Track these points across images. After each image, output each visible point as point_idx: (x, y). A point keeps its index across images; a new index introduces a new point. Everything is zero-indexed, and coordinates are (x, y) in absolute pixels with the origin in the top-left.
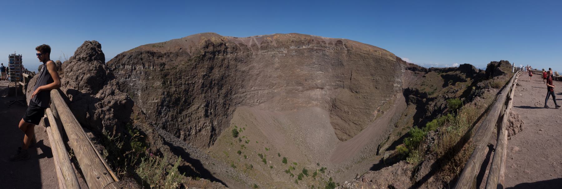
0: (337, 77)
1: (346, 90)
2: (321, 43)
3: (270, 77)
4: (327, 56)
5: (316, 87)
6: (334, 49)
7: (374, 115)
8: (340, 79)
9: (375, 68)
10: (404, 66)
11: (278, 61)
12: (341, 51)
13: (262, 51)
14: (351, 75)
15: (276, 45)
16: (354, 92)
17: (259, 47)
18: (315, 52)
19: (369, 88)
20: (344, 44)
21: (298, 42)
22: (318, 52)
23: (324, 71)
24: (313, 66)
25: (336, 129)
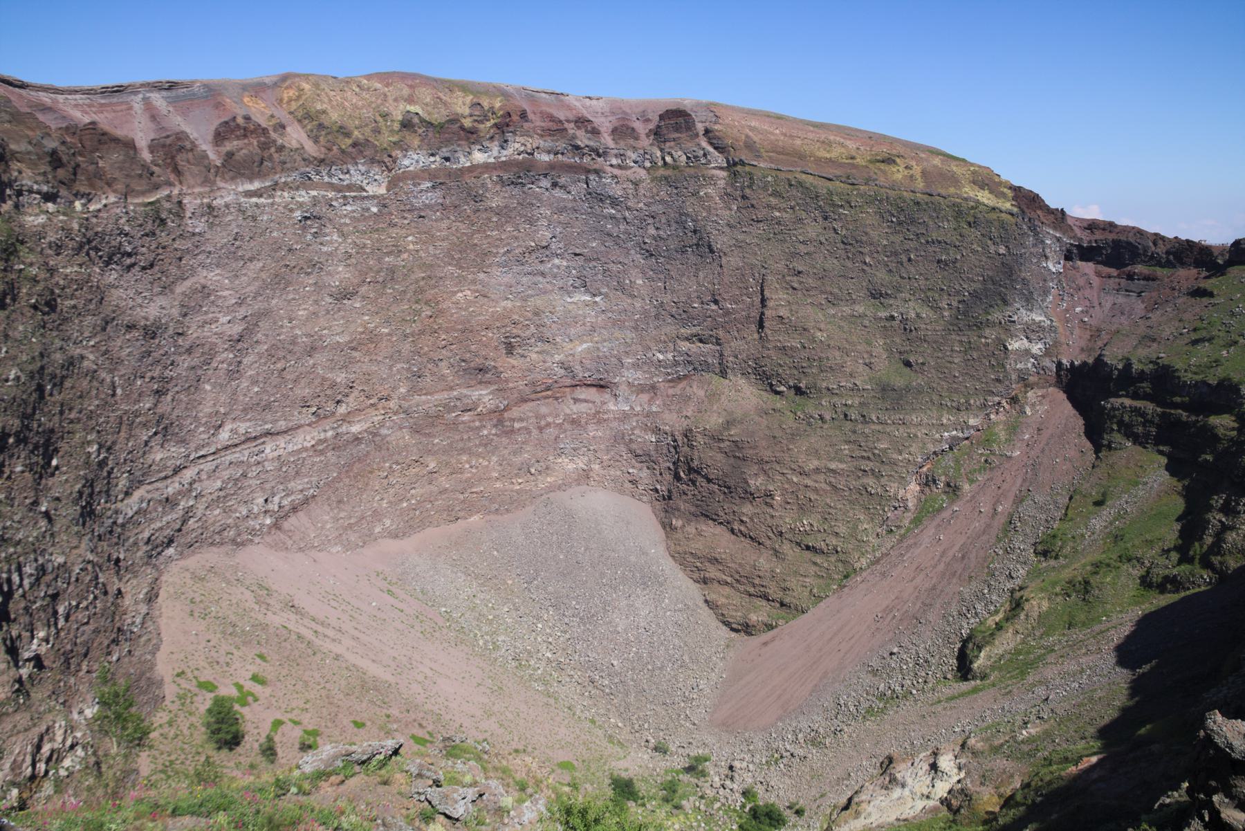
0: (684, 316)
1: (742, 381)
2: (571, 132)
3: (311, 350)
4: (615, 202)
5: (568, 382)
6: (648, 164)
7: (905, 500)
8: (695, 330)
9: (896, 254)
10: (1058, 240)
11: (342, 249)
12: (692, 171)
13: (240, 189)
14: (763, 301)
15: (311, 148)
16: (782, 388)
17: (214, 157)
18: (546, 183)
19: (869, 365)
20: (700, 127)
21: (441, 126)
22: (562, 181)
23: (604, 290)
24: (541, 267)
25: (705, 581)
